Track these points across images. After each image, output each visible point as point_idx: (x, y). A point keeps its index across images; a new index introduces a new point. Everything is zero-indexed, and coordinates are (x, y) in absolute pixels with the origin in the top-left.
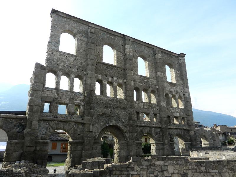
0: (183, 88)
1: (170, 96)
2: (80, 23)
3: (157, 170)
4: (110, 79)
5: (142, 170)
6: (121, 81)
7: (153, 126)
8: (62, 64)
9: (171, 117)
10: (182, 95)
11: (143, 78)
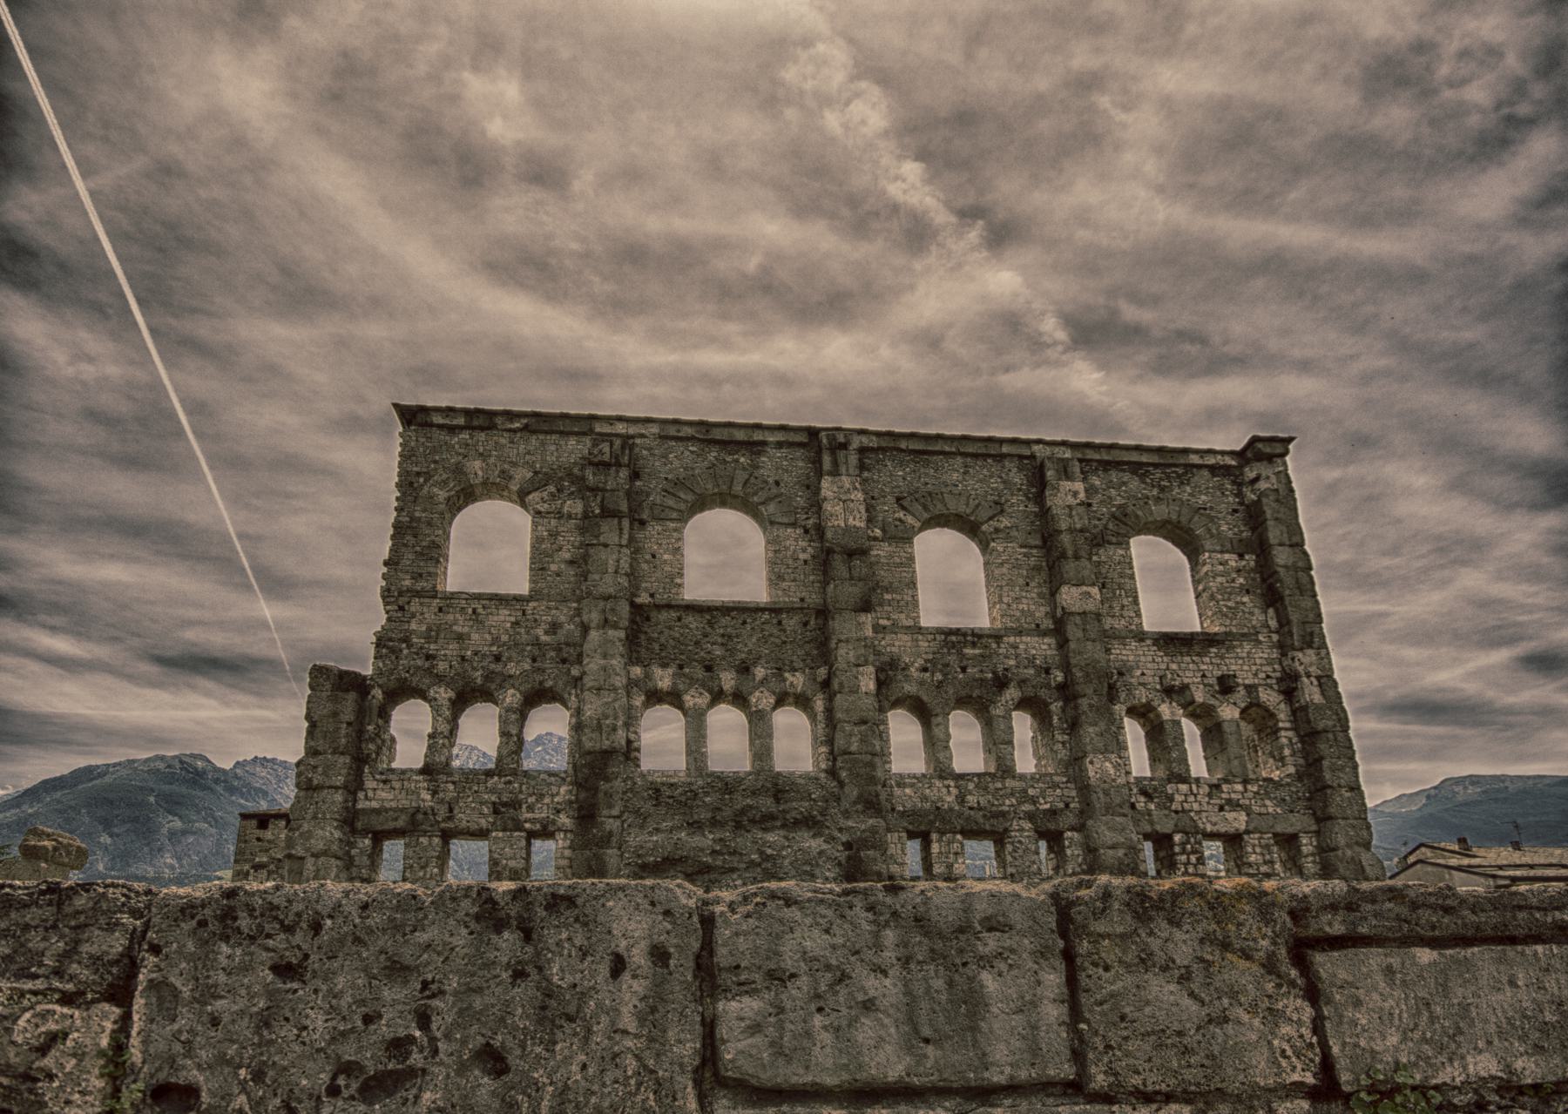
0: (1284, 654)
2: (546, 432)
6: (797, 681)
9: (1177, 838)
10: (1270, 697)
11: (954, 638)
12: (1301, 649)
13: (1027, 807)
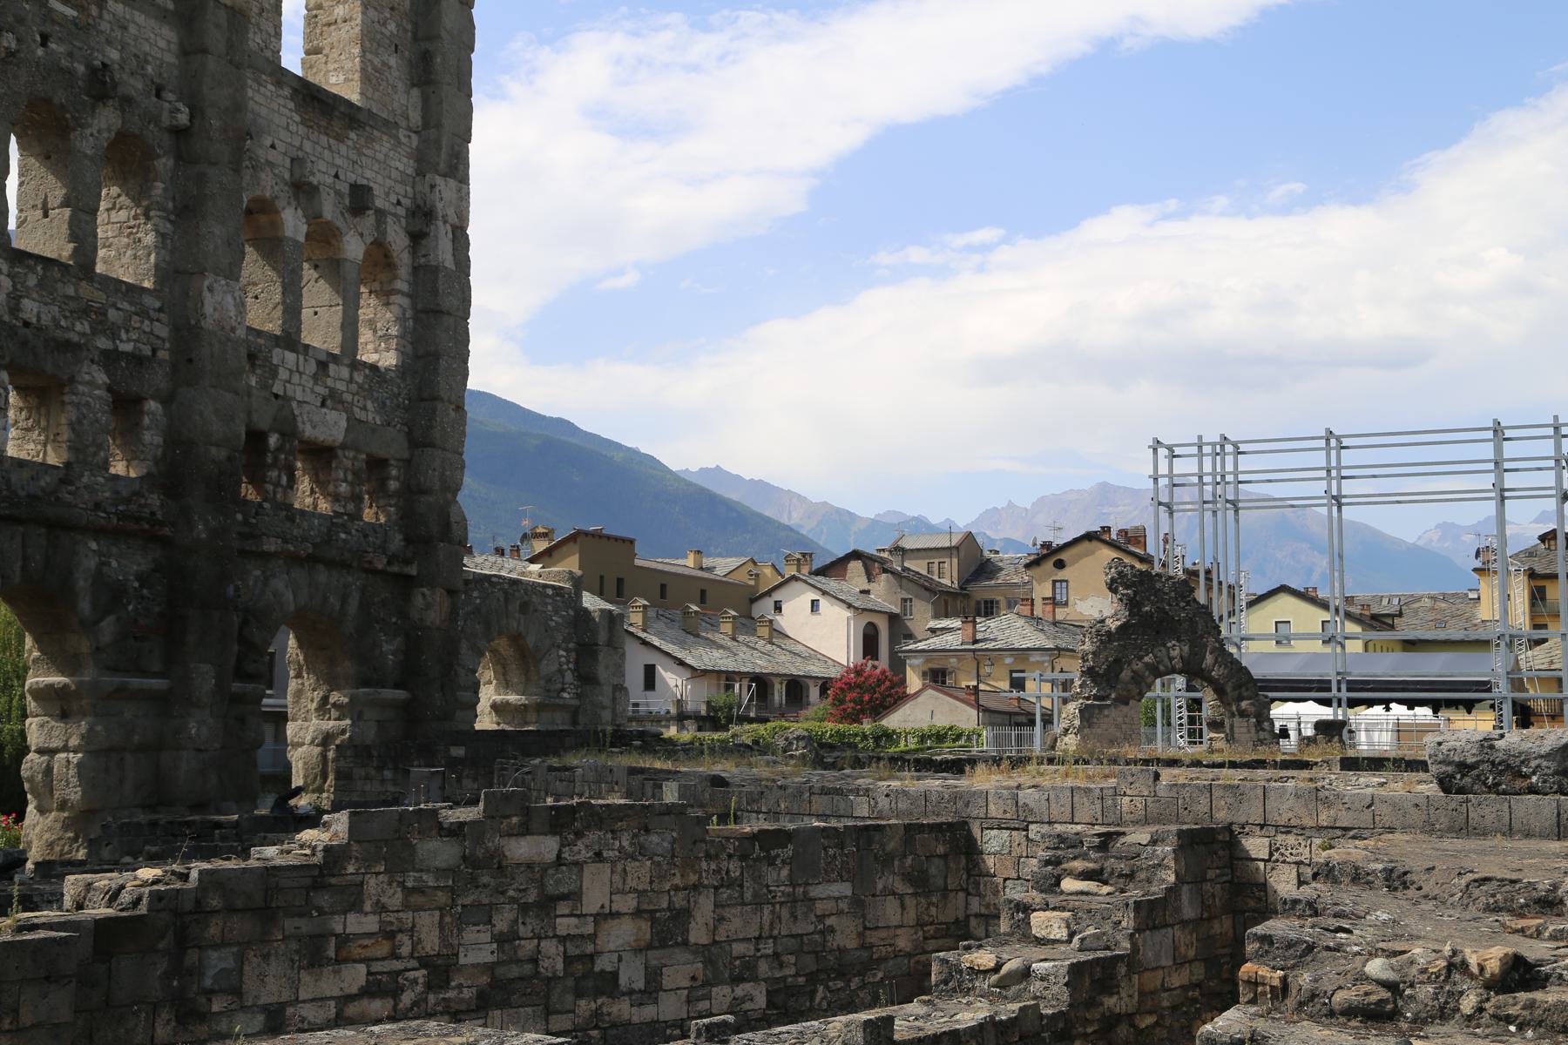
1: (289, 232)
3: (513, 900)
5: (416, 899)
9: (273, 440)
10: (397, 239)
12: (444, 176)
13: (103, 343)
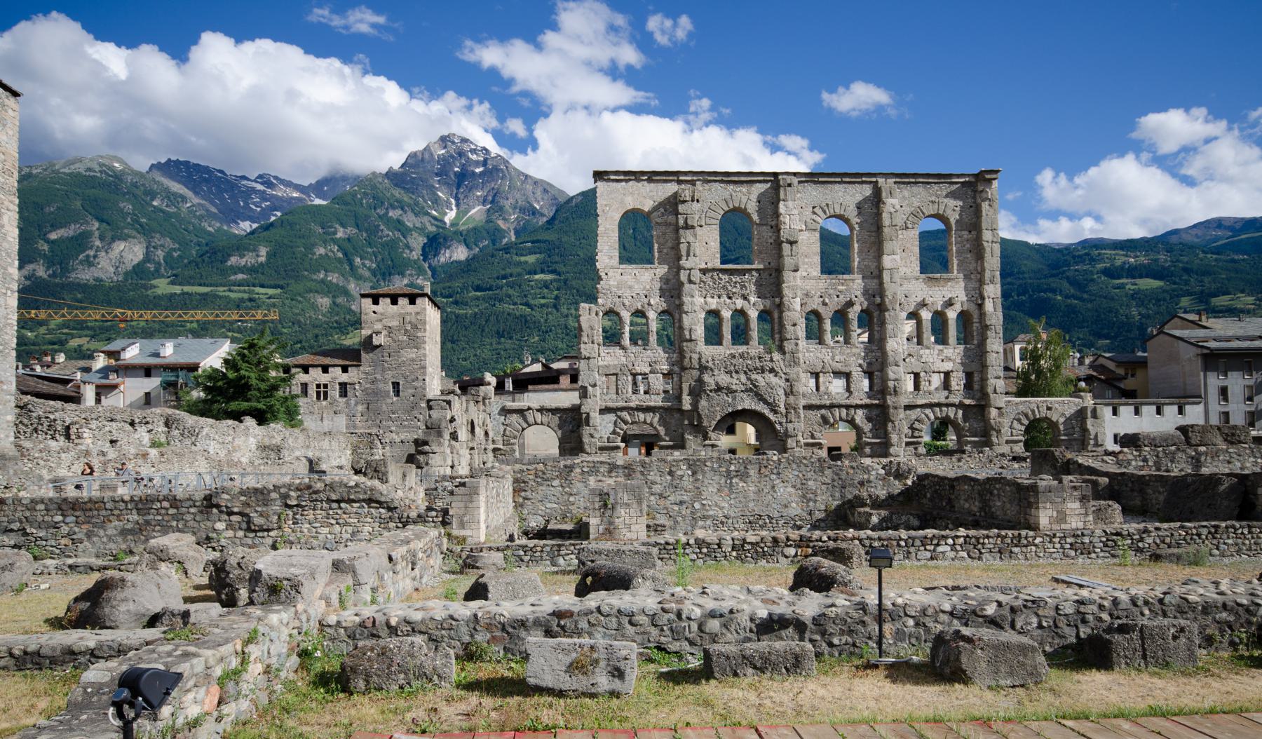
4: (740, 303)
7: (859, 402)
8: (628, 293)
